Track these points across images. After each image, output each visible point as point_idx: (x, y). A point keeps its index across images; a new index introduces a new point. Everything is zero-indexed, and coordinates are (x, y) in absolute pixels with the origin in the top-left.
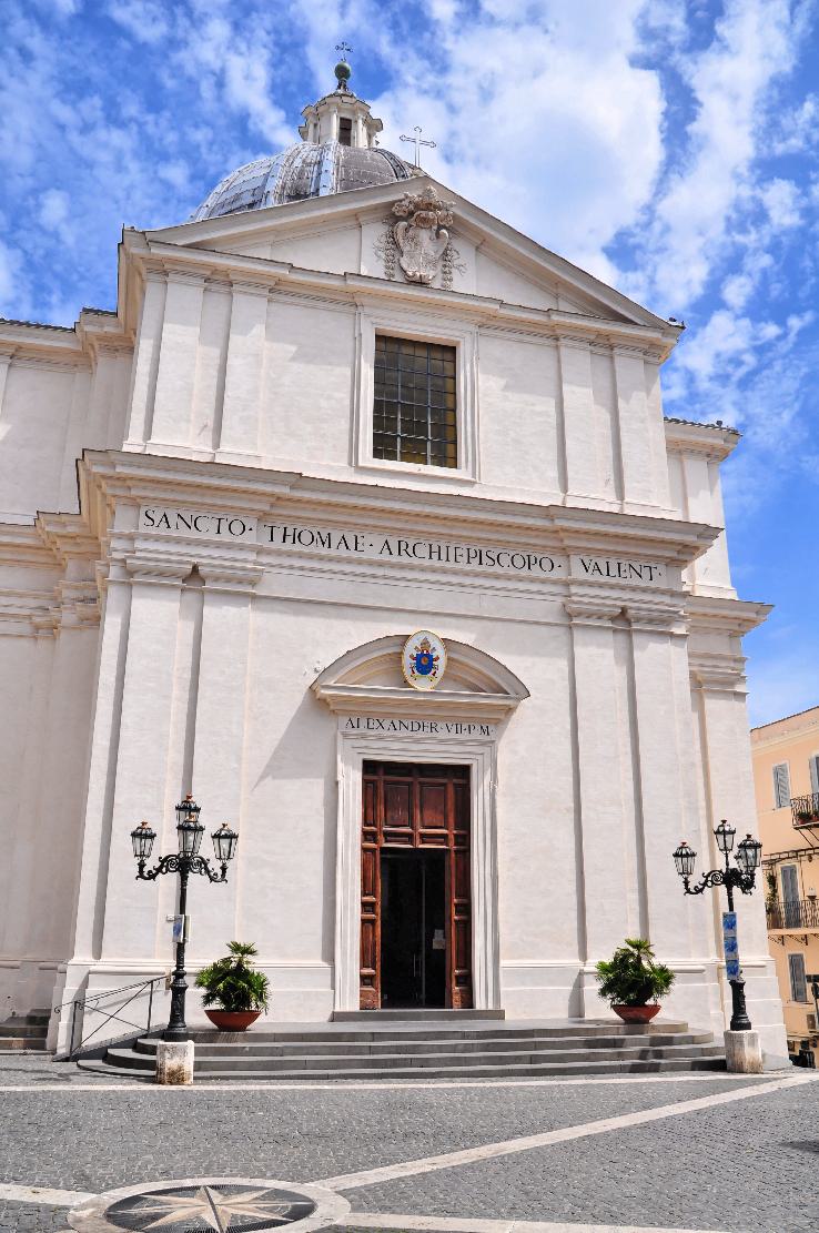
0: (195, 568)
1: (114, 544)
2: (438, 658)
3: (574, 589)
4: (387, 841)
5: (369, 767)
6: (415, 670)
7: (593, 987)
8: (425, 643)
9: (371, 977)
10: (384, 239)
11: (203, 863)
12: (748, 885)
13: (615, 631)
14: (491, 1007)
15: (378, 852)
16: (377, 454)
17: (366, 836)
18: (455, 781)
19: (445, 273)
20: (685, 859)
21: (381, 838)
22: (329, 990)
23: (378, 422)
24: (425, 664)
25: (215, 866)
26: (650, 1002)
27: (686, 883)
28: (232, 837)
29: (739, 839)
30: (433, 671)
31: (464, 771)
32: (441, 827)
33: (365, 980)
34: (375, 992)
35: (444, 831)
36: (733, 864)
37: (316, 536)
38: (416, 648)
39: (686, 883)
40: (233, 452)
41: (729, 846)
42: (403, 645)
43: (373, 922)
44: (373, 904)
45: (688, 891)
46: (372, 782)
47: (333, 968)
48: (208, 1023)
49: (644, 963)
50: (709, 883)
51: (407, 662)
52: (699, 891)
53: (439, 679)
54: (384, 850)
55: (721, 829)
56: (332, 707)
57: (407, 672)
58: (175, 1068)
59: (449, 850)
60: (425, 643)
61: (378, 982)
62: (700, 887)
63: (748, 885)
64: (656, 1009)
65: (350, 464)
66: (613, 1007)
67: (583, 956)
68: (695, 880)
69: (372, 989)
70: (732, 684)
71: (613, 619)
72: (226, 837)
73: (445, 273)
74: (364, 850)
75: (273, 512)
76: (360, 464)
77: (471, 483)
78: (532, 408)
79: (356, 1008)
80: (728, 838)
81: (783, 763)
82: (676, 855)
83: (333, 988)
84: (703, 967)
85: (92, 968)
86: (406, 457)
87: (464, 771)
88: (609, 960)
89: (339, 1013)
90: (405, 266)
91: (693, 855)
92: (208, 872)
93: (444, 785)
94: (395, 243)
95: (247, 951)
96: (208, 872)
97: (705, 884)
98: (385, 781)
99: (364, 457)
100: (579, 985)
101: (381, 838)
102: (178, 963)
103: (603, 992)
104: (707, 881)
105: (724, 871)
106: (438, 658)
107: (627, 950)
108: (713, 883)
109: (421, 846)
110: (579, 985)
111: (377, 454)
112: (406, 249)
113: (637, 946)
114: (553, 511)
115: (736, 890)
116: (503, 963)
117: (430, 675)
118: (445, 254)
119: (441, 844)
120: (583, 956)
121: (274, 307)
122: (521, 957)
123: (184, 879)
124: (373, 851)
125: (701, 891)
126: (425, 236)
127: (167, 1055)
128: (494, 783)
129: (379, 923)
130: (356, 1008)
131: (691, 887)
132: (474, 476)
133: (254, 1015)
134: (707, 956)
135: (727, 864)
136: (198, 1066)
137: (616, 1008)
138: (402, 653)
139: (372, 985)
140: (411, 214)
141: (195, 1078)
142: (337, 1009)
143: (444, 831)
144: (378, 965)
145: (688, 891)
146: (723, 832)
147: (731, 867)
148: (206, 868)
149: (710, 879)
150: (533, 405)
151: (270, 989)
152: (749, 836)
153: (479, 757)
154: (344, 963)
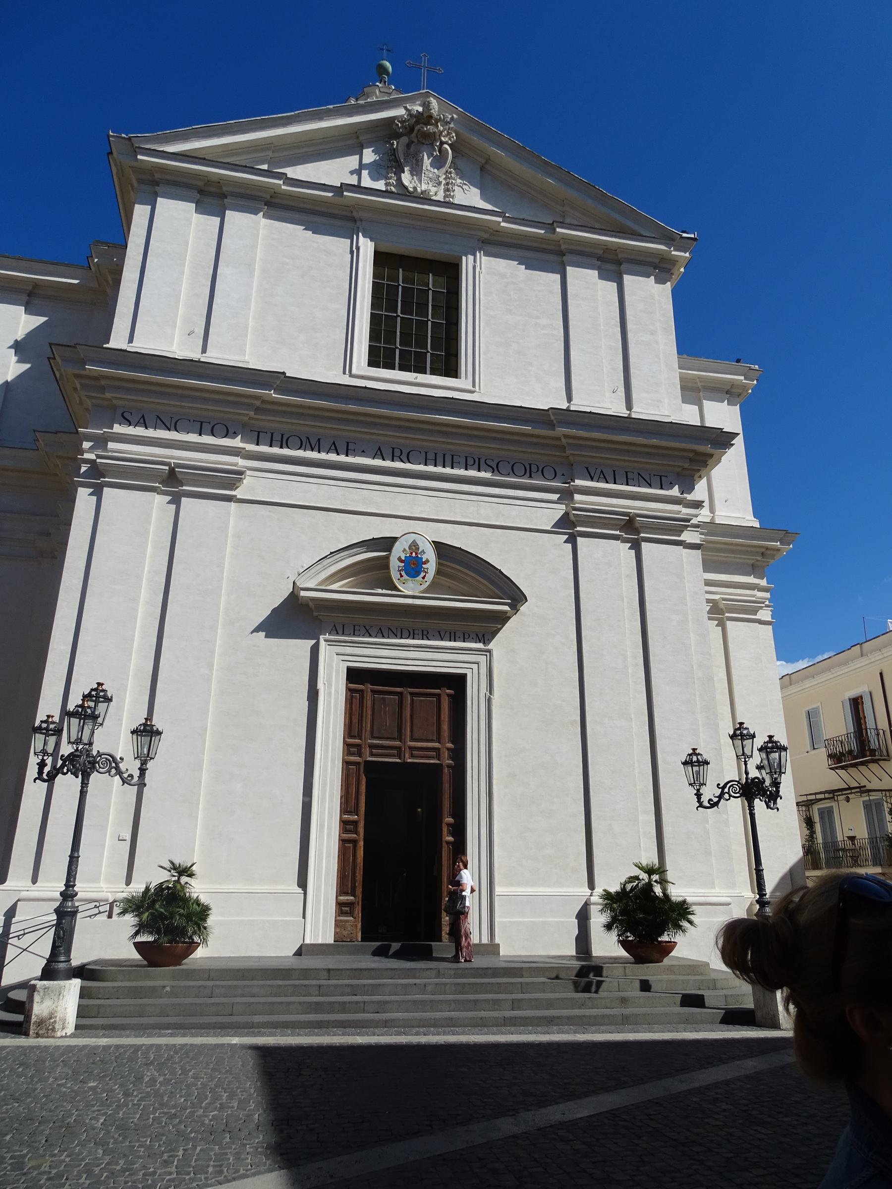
0: (172, 471)
1: (86, 445)
2: (427, 561)
4: (372, 755)
5: (354, 675)
6: (403, 573)
7: (598, 919)
8: (414, 546)
9: (350, 904)
11: (113, 764)
12: (773, 798)
14: (485, 940)
16: (371, 363)
17: (348, 747)
18: (448, 691)
19: (448, 190)
20: (695, 769)
21: (366, 751)
22: (301, 919)
23: (374, 334)
24: (414, 566)
26: (665, 938)
27: (699, 795)
29: (759, 742)
30: (422, 574)
31: (457, 683)
32: (432, 741)
33: (342, 908)
34: (354, 923)
35: (436, 745)
36: (754, 773)
37: (304, 440)
38: (404, 550)
39: (699, 795)
40: (216, 355)
41: (748, 751)
42: (389, 549)
43: (354, 842)
44: (355, 823)
45: (701, 805)
46: (361, 692)
47: (305, 894)
48: (135, 955)
49: (658, 890)
50: (727, 796)
51: (395, 564)
52: (713, 805)
53: (428, 583)
54: (366, 762)
55: (738, 732)
56: (315, 614)
57: (394, 575)
58: (45, 1014)
59: (441, 765)
60: (414, 546)
61: (358, 911)
62: (716, 800)
63: (773, 798)
64: (671, 946)
65: (344, 373)
66: (619, 941)
67: (591, 885)
68: (710, 792)
69: (352, 918)
74: (346, 763)
76: (354, 371)
77: (472, 392)
78: (538, 321)
79: (331, 940)
80: (748, 743)
81: (815, 706)
82: (685, 763)
83: (304, 917)
84: (728, 900)
85: (24, 894)
86: (403, 368)
87: (457, 683)
88: (614, 888)
89: (308, 945)
91: (707, 763)
92: (119, 772)
95: (185, 871)
96: (119, 772)
97: (720, 797)
98: (372, 691)
99: (359, 362)
100: (583, 916)
101: (366, 751)
102: (68, 880)
103: (609, 927)
104: (722, 794)
105: (744, 781)
106: (427, 561)
107: (637, 878)
108: (730, 796)
109: (409, 760)
110: (583, 916)
111: (371, 363)
113: (650, 871)
115: (759, 805)
116: (498, 890)
117: (420, 578)
119: (432, 757)
120: (591, 885)
122: (519, 884)
123: (84, 784)
124: (357, 764)
125: (716, 804)
127: (37, 998)
128: (491, 693)
129: (361, 843)
130: (331, 940)
131: (705, 800)
132: (474, 386)
133: (192, 947)
134: (733, 886)
135: (747, 773)
136: (82, 1012)
137: (625, 944)
138: (387, 558)
139: (351, 914)
140: (412, 129)
141: (77, 1027)
142: (307, 941)
143: (436, 745)
144: (359, 891)
145: (701, 805)
146: (740, 734)
147: (751, 776)
148: (117, 768)
149: (726, 790)
150: (538, 318)
151: (211, 921)
152: (771, 737)
153: (475, 666)
154: (318, 889)
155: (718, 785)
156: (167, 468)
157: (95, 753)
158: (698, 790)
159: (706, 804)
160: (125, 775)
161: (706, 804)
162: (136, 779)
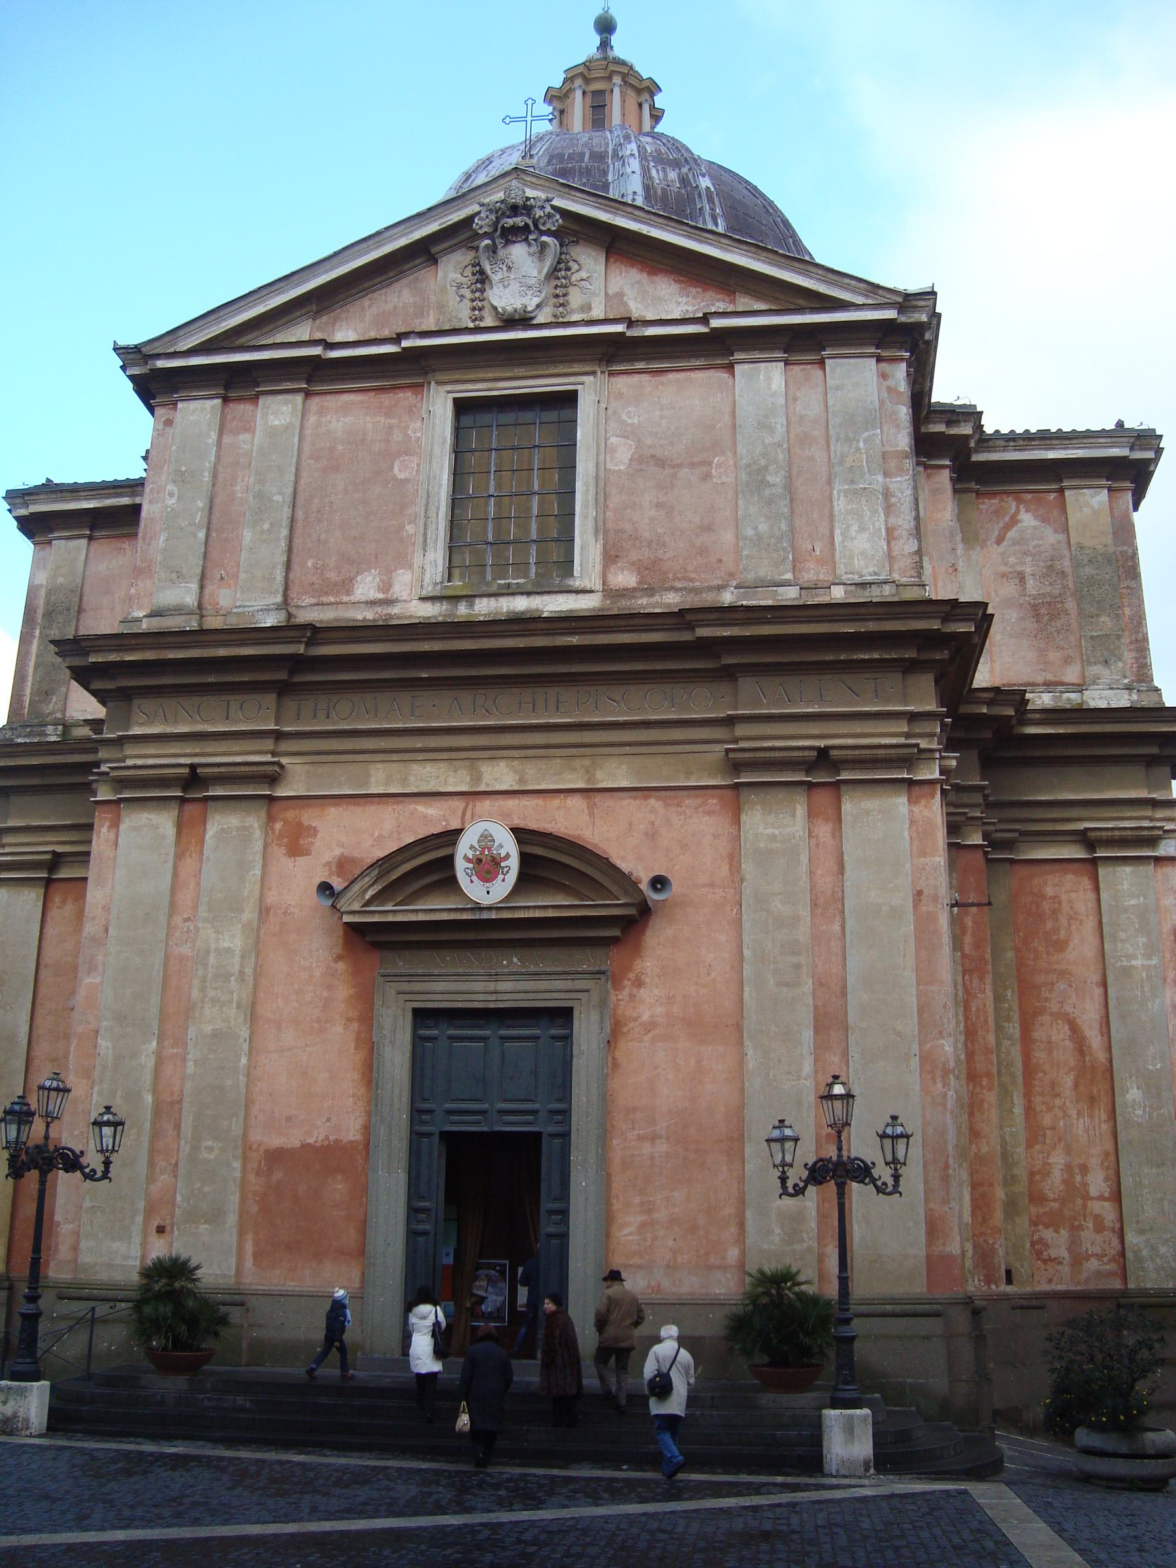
2: (507, 856)
3: (740, 730)
5: (422, 1016)
6: (474, 878)
10: (469, 270)
13: (810, 786)
15: (436, 1139)
25: (93, 1160)
28: (117, 1124)
39: (783, 1179)
45: (785, 1192)
62: (802, 1185)
70: (1152, 842)
71: (809, 766)
72: (108, 1123)
73: (557, 296)
75: (298, 679)
90: (495, 303)
93: (535, 1038)
94: (482, 272)
106: (507, 856)
112: (495, 278)
114: (689, 617)
118: (553, 273)
121: (315, 402)
126: (518, 252)
136: (53, 1414)
155: (806, 1165)
156: (187, 770)
157: (51, 1148)
158: (784, 1172)
159: (791, 1190)
160: (87, 1170)
161: (791, 1190)
162: (99, 1174)
